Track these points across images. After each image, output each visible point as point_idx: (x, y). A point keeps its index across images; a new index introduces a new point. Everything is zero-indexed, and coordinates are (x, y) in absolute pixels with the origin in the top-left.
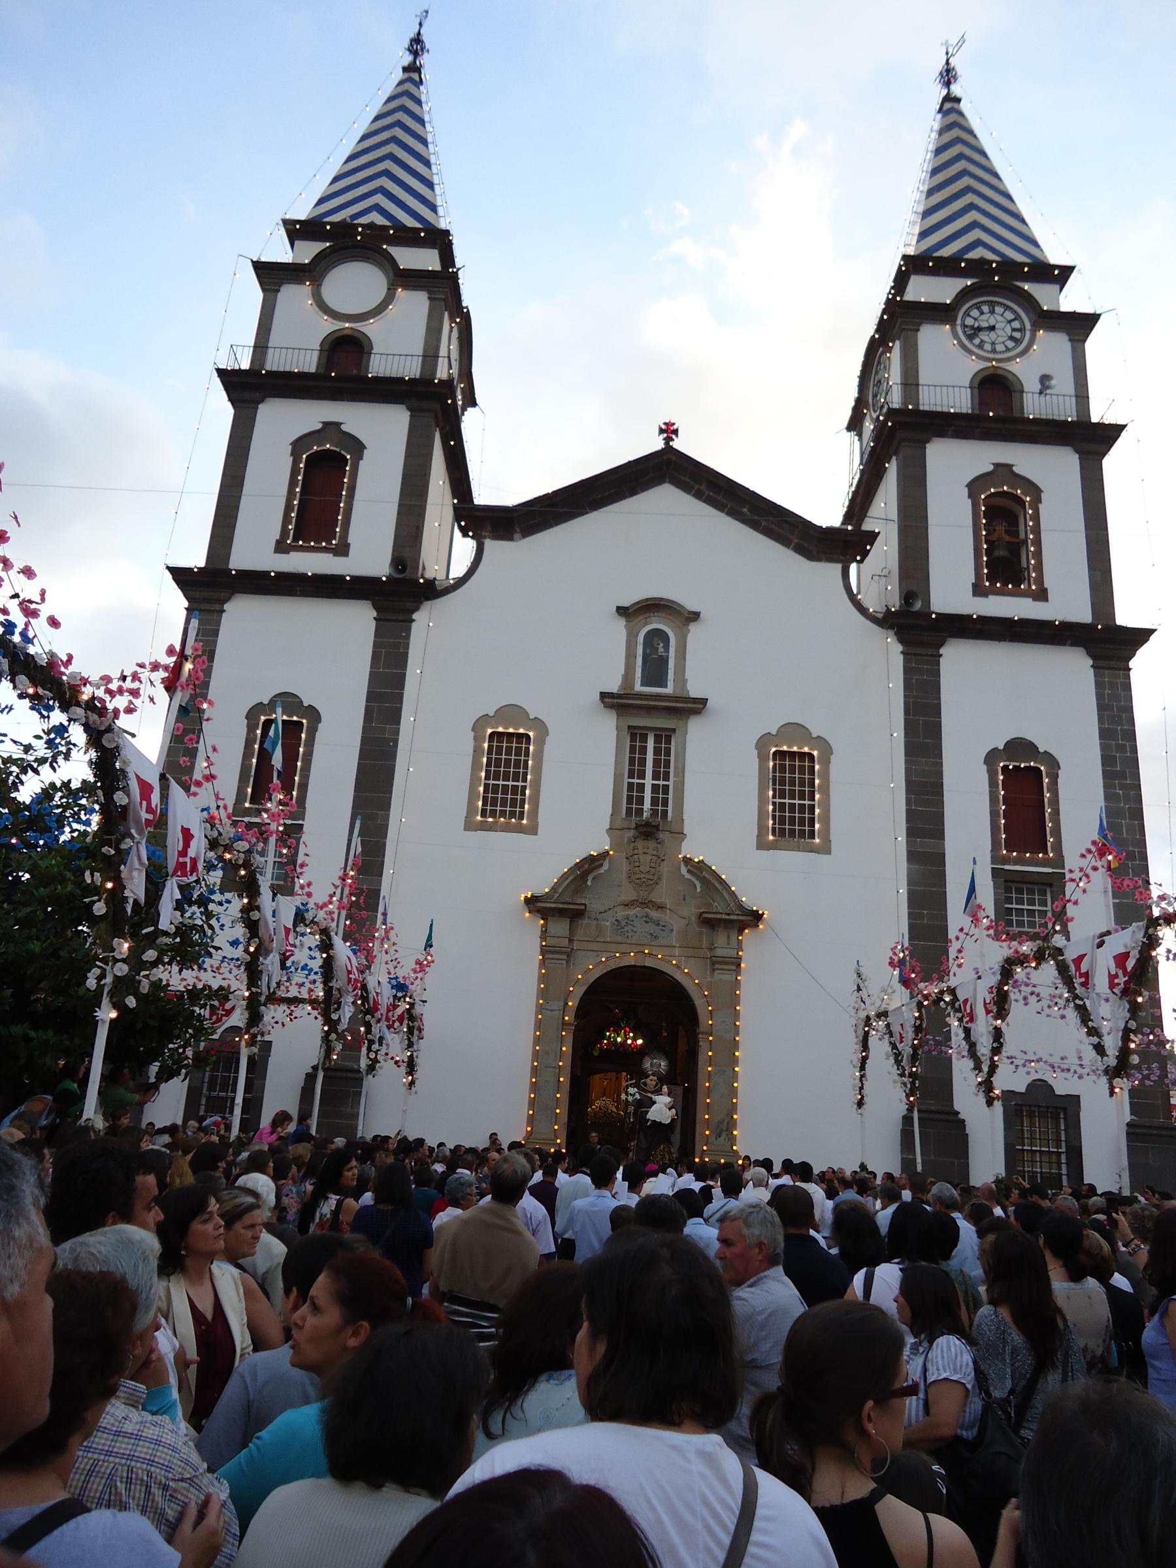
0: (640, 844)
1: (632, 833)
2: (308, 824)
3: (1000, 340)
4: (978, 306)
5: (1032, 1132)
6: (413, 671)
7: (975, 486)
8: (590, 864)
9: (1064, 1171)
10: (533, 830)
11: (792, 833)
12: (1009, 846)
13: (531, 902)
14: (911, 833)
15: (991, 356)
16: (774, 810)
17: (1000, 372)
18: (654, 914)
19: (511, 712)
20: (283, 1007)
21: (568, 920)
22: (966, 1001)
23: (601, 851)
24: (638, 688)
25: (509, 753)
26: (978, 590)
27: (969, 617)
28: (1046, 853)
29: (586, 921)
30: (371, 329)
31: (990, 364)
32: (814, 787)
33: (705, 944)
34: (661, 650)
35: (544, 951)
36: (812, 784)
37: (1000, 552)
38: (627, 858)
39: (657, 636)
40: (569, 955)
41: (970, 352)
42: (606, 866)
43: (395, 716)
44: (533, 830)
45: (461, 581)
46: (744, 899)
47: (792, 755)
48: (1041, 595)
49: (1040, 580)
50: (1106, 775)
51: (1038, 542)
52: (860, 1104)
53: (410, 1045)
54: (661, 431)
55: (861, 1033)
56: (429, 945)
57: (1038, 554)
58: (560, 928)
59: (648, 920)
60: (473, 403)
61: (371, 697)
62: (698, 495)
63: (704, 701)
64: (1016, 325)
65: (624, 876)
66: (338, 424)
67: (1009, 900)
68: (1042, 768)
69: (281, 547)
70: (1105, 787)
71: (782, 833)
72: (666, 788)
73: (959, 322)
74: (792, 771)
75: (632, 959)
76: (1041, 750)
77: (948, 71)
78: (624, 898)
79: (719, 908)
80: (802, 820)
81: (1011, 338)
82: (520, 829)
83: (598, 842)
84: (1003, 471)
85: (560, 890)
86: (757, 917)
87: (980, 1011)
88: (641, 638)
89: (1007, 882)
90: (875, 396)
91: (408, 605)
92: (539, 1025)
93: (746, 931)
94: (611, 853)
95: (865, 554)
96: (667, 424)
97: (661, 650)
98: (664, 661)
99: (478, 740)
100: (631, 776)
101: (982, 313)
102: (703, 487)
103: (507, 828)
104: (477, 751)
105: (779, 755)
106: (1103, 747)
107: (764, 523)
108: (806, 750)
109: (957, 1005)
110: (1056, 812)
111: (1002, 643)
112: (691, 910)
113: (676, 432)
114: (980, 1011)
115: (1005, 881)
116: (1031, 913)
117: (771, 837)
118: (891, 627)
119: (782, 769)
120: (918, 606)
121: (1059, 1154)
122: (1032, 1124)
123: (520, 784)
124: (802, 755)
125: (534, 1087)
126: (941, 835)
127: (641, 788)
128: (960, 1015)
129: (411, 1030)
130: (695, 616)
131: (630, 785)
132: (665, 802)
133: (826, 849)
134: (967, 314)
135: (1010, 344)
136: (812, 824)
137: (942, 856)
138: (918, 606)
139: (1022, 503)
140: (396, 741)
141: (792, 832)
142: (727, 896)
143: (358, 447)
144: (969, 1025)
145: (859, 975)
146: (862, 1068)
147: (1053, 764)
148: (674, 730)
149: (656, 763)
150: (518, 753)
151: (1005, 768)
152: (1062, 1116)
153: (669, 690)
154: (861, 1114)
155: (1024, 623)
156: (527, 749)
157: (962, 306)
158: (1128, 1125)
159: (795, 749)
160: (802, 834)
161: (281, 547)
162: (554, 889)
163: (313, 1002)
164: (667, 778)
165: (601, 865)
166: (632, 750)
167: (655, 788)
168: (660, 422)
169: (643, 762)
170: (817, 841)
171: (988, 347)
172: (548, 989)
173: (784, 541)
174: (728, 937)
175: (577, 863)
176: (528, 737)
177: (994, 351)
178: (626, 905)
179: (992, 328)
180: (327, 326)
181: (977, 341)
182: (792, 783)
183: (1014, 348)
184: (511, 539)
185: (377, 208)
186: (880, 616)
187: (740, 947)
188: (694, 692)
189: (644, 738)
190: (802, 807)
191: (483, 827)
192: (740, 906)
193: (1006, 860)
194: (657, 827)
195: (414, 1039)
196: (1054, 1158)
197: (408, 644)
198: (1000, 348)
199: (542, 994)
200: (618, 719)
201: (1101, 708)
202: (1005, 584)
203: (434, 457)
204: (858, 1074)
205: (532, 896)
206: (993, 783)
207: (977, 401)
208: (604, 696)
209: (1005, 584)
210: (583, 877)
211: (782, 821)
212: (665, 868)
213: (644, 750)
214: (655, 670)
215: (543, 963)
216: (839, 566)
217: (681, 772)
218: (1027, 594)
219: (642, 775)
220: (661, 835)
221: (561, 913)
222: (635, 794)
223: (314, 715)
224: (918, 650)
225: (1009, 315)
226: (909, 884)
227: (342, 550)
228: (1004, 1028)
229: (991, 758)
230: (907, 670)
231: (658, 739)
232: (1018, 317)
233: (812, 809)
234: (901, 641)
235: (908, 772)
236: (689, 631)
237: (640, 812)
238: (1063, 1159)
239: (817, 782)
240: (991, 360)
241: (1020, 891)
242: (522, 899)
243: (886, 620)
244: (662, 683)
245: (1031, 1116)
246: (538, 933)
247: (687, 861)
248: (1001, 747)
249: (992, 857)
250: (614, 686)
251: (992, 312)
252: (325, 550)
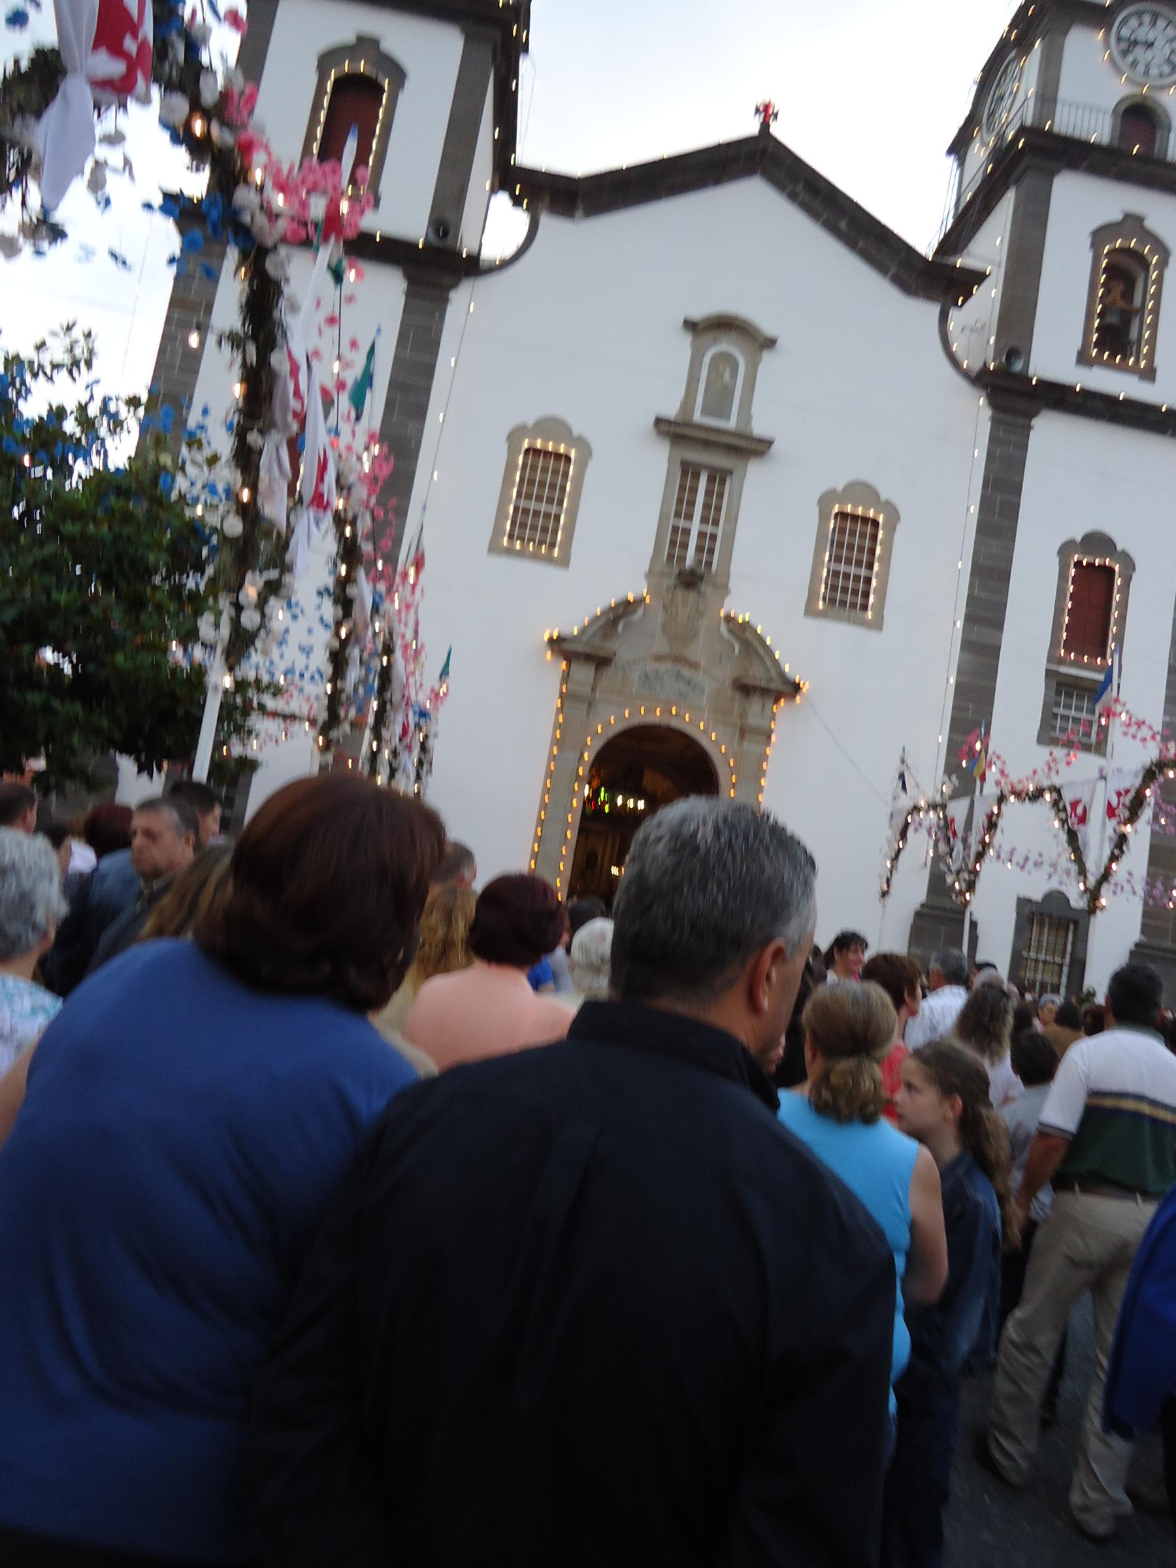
0: (680, 593)
1: (671, 581)
4: (1139, 14)
5: (1039, 941)
6: (446, 361)
7: (1100, 235)
8: (624, 609)
9: (1064, 980)
11: (843, 603)
12: (1068, 647)
13: (556, 644)
14: (970, 619)
16: (828, 575)
17: (1149, 102)
18: (686, 672)
19: (552, 426)
20: (279, 722)
21: (594, 668)
22: (1074, 805)
23: (638, 595)
24: (697, 417)
25: (545, 470)
26: (1083, 359)
27: (1071, 389)
28: (1104, 657)
29: (610, 671)
32: (873, 553)
33: (736, 708)
34: (727, 375)
35: (562, 696)
36: (872, 551)
37: (1113, 319)
38: (665, 608)
39: (726, 359)
40: (590, 705)
41: (1120, 72)
43: (420, 412)
44: (564, 562)
45: (506, 264)
46: (787, 669)
47: (855, 518)
48: (1149, 374)
49: (1151, 356)
51: (1156, 311)
52: (884, 894)
53: (418, 778)
55: (900, 823)
56: (445, 673)
57: (1154, 326)
58: (584, 673)
59: (678, 676)
62: (793, 197)
63: (769, 443)
65: (659, 625)
67: (1058, 704)
68: (1117, 568)
71: (832, 601)
72: (713, 537)
74: (853, 533)
75: (657, 716)
76: (1119, 547)
79: (756, 675)
80: (855, 592)
82: (549, 559)
83: (635, 587)
84: (1133, 223)
85: (590, 632)
86: (796, 688)
87: (1097, 813)
90: (992, 114)
92: (549, 774)
93: (782, 701)
94: (648, 601)
95: (968, 295)
97: (727, 375)
98: (729, 392)
99: (512, 452)
100: (678, 515)
102: (800, 187)
103: (536, 556)
104: (510, 467)
105: (842, 516)
107: (860, 244)
108: (871, 514)
109: (1061, 805)
110: (1123, 618)
111: (1099, 421)
112: (726, 673)
114: (1097, 813)
115: (1057, 684)
116: (1076, 720)
117: (821, 605)
118: (985, 387)
119: (842, 531)
120: (1018, 366)
121: (1061, 966)
122: (1041, 933)
123: (554, 510)
124: (865, 520)
125: (539, 839)
126: (999, 625)
127: (687, 532)
128: (1063, 815)
129: (420, 763)
130: (770, 343)
131: (675, 529)
132: (711, 551)
133: (877, 624)
134: (1125, 21)
136: (866, 595)
137: (999, 648)
138: (1018, 366)
139: (1145, 264)
140: (419, 443)
141: (843, 603)
142: (768, 663)
144: (1076, 827)
145: (903, 761)
146: (895, 858)
147: (1129, 565)
148: (731, 473)
149: (707, 507)
150: (555, 472)
151: (1078, 564)
152: (1071, 927)
153: (732, 424)
154: (884, 906)
155: (1129, 403)
156: (566, 474)
158: (1137, 945)
159: (860, 511)
160: (853, 605)
162: (583, 631)
163: (313, 723)
164: (716, 522)
165: (635, 611)
166: (682, 488)
167: (701, 535)
168: (760, 100)
169: (692, 503)
170: (870, 614)
172: (565, 738)
173: (881, 268)
174: (764, 704)
175: (611, 608)
176: (568, 459)
178: (658, 658)
179: (1150, 45)
181: (1130, 58)
186: (974, 375)
187: (773, 717)
188: (759, 428)
189: (696, 476)
190: (857, 578)
191: (509, 551)
192: (782, 675)
193: (1061, 661)
194: (701, 578)
195: (424, 772)
196: (1056, 968)
197: (440, 331)
199: (556, 742)
200: (670, 452)
202: (1113, 356)
203: (487, 100)
204: (889, 865)
205: (559, 637)
206: (1063, 576)
207: (1118, 134)
208: (659, 422)
209: (1113, 356)
210: (614, 622)
211: (834, 588)
212: (704, 624)
213: (694, 490)
215: (561, 710)
216: (934, 309)
217: (733, 520)
218: (1135, 370)
219: (689, 517)
220: (705, 587)
221: (588, 658)
222: (678, 538)
224: (1008, 418)
228: (1131, 838)
229: (1066, 550)
230: (993, 439)
231: (711, 480)
233: (868, 581)
234: (993, 403)
235: (976, 553)
236: (760, 360)
237: (682, 559)
238: (1065, 970)
239: (878, 551)
241: (1069, 695)
242: (546, 637)
243: (981, 379)
244: (724, 414)
245: (1041, 925)
246: (558, 676)
247: (729, 619)
248: (1078, 538)
249: (1048, 657)
250: (671, 410)
251: (1154, 23)
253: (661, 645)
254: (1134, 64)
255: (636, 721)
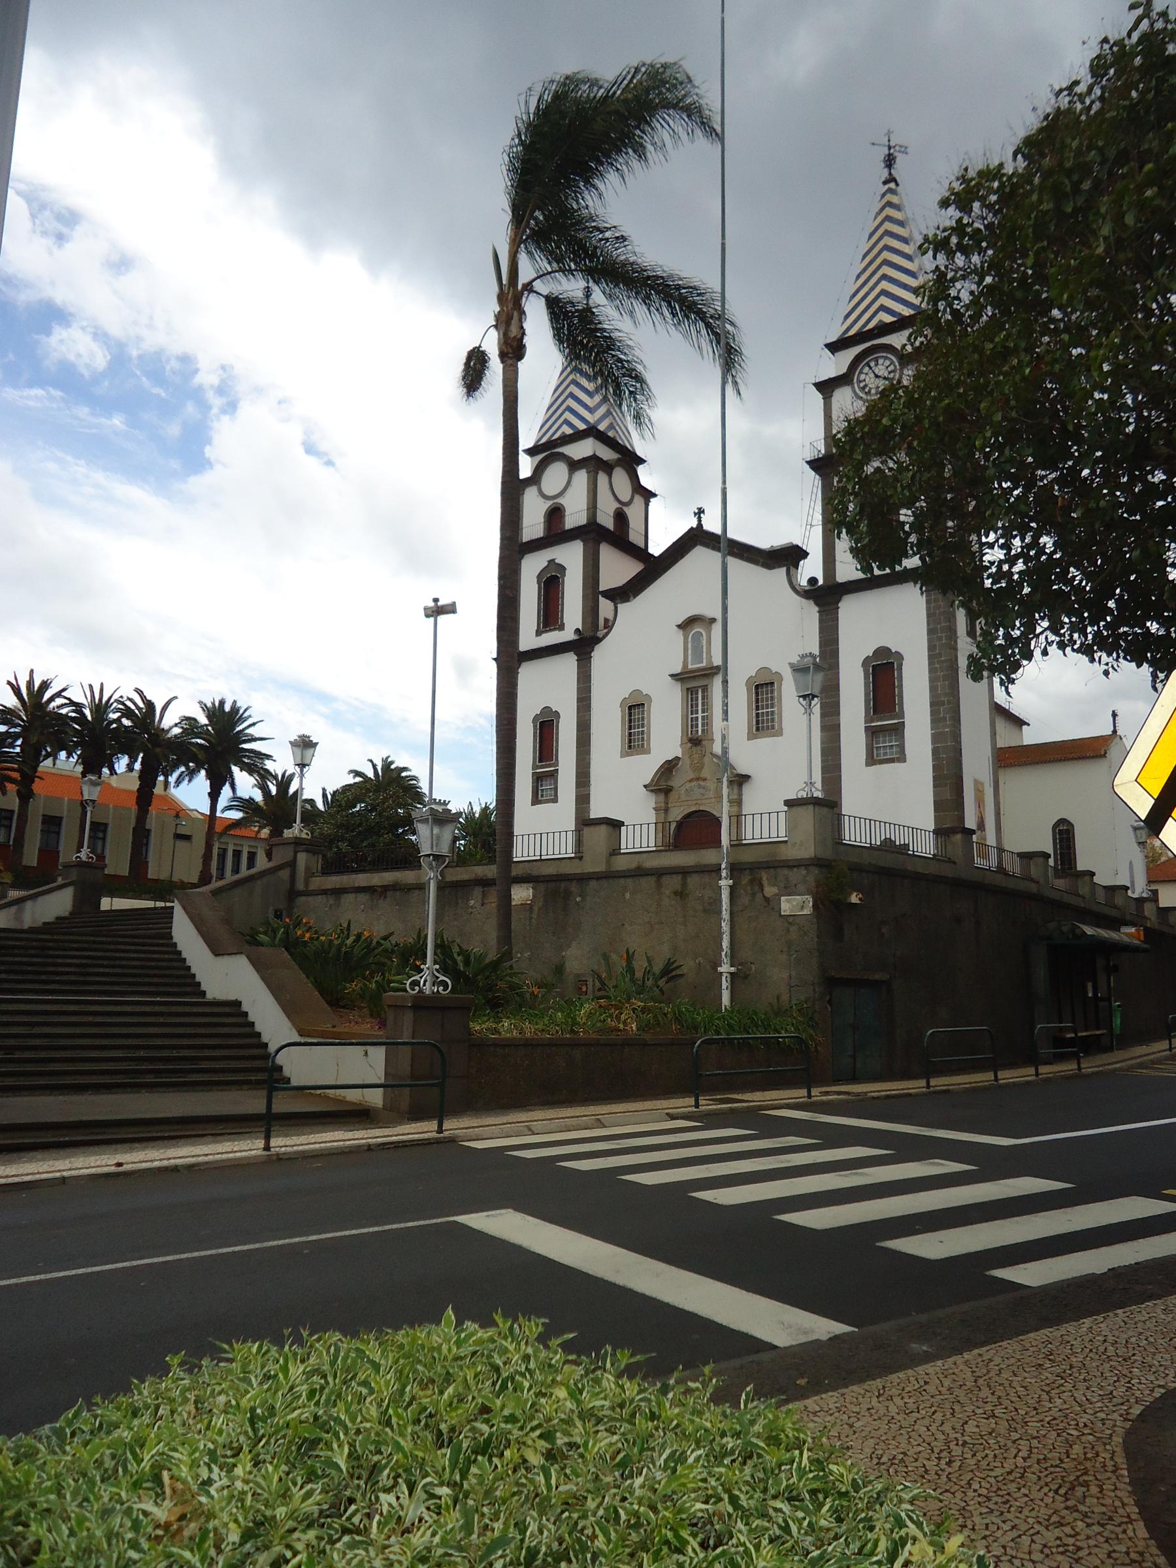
0: (694, 749)
2: (560, 768)
10: (648, 752)
18: (702, 783)
30: (560, 500)
42: (680, 763)
44: (648, 752)
50: (930, 657)
54: (695, 514)
59: (700, 787)
60: (654, 495)
61: (579, 700)
66: (553, 560)
69: (539, 633)
70: (930, 664)
73: (855, 380)
77: (890, 155)
78: (688, 778)
83: (678, 752)
88: (690, 639)
89: (873, 733)
91: (589, 650)
96: (699, 509)
101: (870, 368)
106: (929, 641)
113: (703, 512)
133: (780, 733)
134: (861, 372)
143: (562, 569)
147: (899, 656)
153: (704, 665)
157: (856, 369)
161: (539, 633)
162: (652, 780)
167: (703, 717)
169: (697, 705)
180: (545, 505)
181: (867, 390)
182: (767, 699)
184: (628, 601)
185: (567, 422)
191: (628, 755)
201: (929, 616)
208: (672, 676)
212: (706, 760)
213: (697, 699)
214: (698, 655)
220: (704, 742)
223: (557, 714)
225: (887, 363)
226: (822, 743)
227: (561, 627)
230: (821, 621)
231: (703, 692)
232: (892, 363)
234: (817, 604)
250: (678, 669)
252: (555, 629)
253: (691, 775)
254: (869, 391)
255: (686, 812)
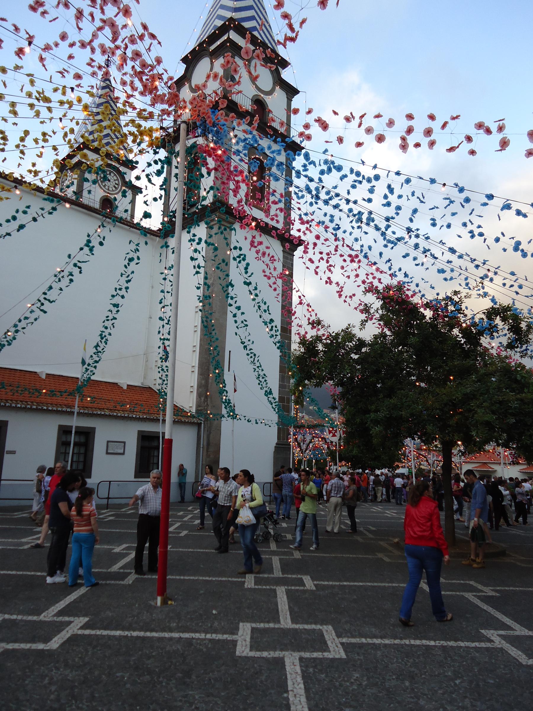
3: (111, 186)
15: (107, 191)
31: (107, 194)
41: (101, 188)
64: (117, 182)
81: (115, 187)
135: (114, 189)
171: (107, 187)
177: (108, 189)
179: (109, 181)
181: (104, 184)
183: (115, 191)
198: (111, 189)
225: (116, 179)
232: (118, 180)
240: (108, 193)
254: (104, 186)
